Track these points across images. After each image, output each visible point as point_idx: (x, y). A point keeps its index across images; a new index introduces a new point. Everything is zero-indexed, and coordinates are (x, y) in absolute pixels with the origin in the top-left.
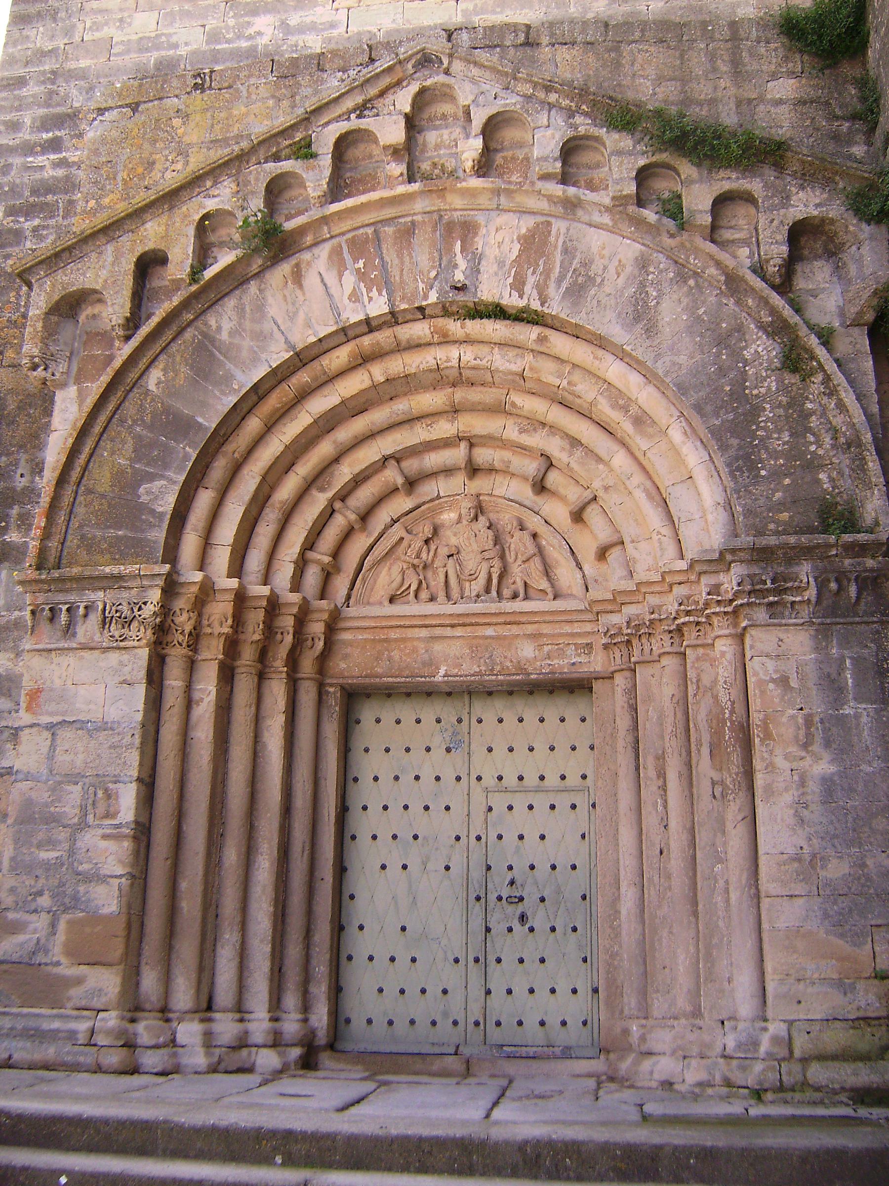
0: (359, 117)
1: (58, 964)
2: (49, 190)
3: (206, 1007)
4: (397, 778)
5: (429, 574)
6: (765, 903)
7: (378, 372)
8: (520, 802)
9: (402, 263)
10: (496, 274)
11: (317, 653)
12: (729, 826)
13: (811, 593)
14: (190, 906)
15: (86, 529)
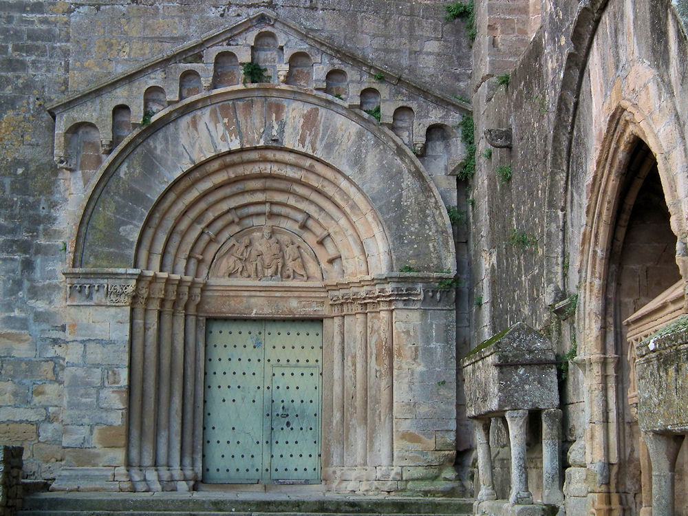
0: (229, 44)
1: (95, 447)
2: (37, 39)
3: (156, 464)
4: (230, 360)
5: (247, 263)
6: (395, 421)
7: (232, 174)
8: (288, 372)
9: (247, 122)
10: (292, 133)
11: (197, 303)
12: (382, 389)
13: (421, 297)
14: (149, 422)
15: (93, 247)
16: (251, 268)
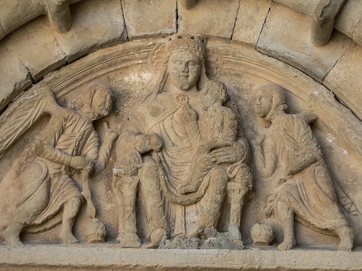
5: (101, 188)
16: (116, 203)
